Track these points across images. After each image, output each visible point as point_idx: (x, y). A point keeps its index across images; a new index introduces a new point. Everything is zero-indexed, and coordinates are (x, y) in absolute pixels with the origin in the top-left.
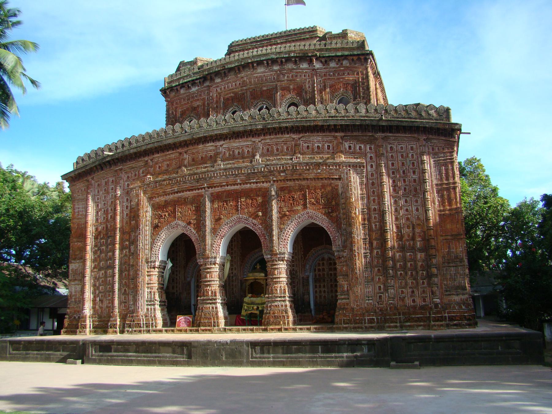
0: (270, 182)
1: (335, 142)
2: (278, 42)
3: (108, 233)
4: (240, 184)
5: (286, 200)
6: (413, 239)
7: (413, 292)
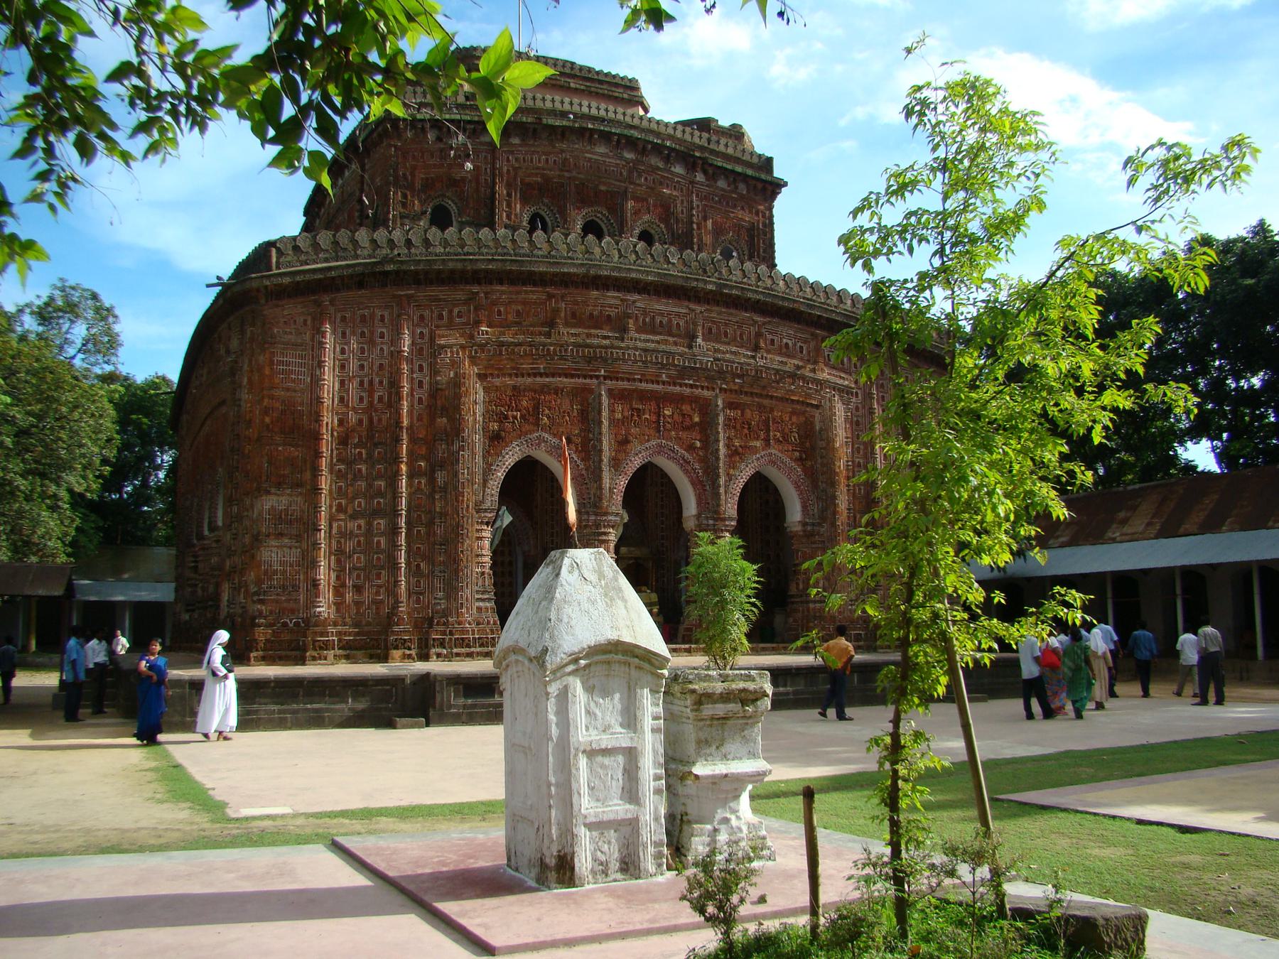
0: (713, 389)
1: (812, 344)
2: (572, 85)
3: (373, 436)
4: (664, 383)
5: (738, 427)
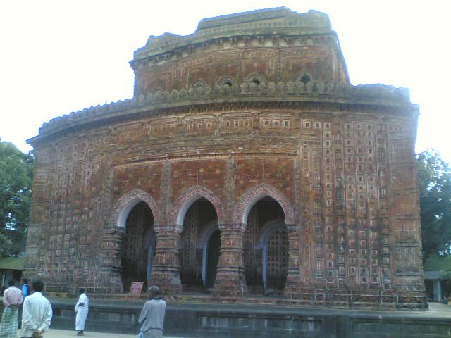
1: (293, 119)
6: (366, 217)
7: (363, 270)
